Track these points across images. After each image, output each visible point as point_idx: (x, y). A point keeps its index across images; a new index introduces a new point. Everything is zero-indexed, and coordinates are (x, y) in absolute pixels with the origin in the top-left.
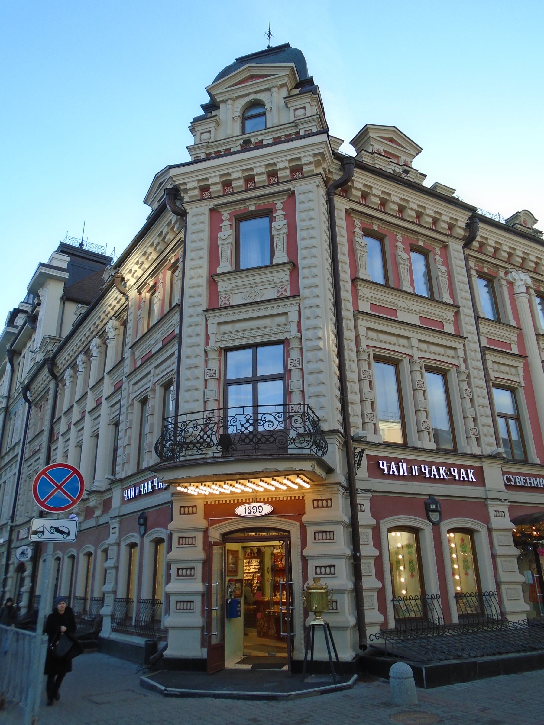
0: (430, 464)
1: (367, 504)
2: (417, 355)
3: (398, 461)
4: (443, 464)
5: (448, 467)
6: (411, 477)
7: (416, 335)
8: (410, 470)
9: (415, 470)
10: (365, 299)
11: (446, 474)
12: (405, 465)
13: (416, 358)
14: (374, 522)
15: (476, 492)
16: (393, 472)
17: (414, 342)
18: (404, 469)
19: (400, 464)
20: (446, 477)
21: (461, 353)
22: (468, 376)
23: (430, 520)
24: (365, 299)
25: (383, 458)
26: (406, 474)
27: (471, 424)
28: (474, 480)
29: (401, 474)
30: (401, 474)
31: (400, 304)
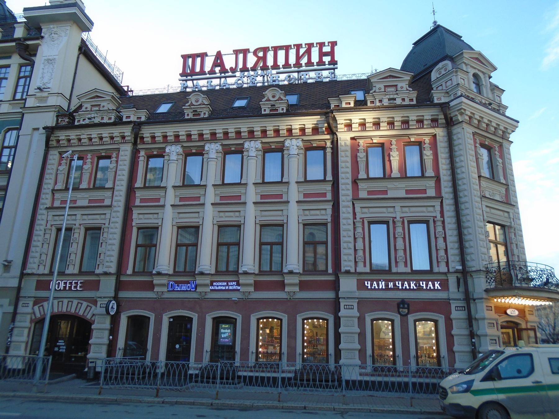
0: (403, 281)
1: (355, 305)
2: (398, 216)
3: (378, 281)
4: (413, 280)
5: (418, 281)
6: (387, 288)
7: (398, 204)
8: (387, 285)
9: (391, 285)
10: (364, 189)
11: (416, 286)
12: (383, 282)
13: (398, 218)
14: (358, 315)
15: (443, 295)
16: (375, 287)
17: (398, 209)
18: (382, 285)
19: (380, 282)
20: (415, 288)
21: (438, 208)
22: (443, 222)
23: (399, 313)
24: (364, 189)
25: (368, 280)
26: (384, 287)
27: (442, 253)
28: (439, 288)
29: (380, 287)
30: (380, 287)
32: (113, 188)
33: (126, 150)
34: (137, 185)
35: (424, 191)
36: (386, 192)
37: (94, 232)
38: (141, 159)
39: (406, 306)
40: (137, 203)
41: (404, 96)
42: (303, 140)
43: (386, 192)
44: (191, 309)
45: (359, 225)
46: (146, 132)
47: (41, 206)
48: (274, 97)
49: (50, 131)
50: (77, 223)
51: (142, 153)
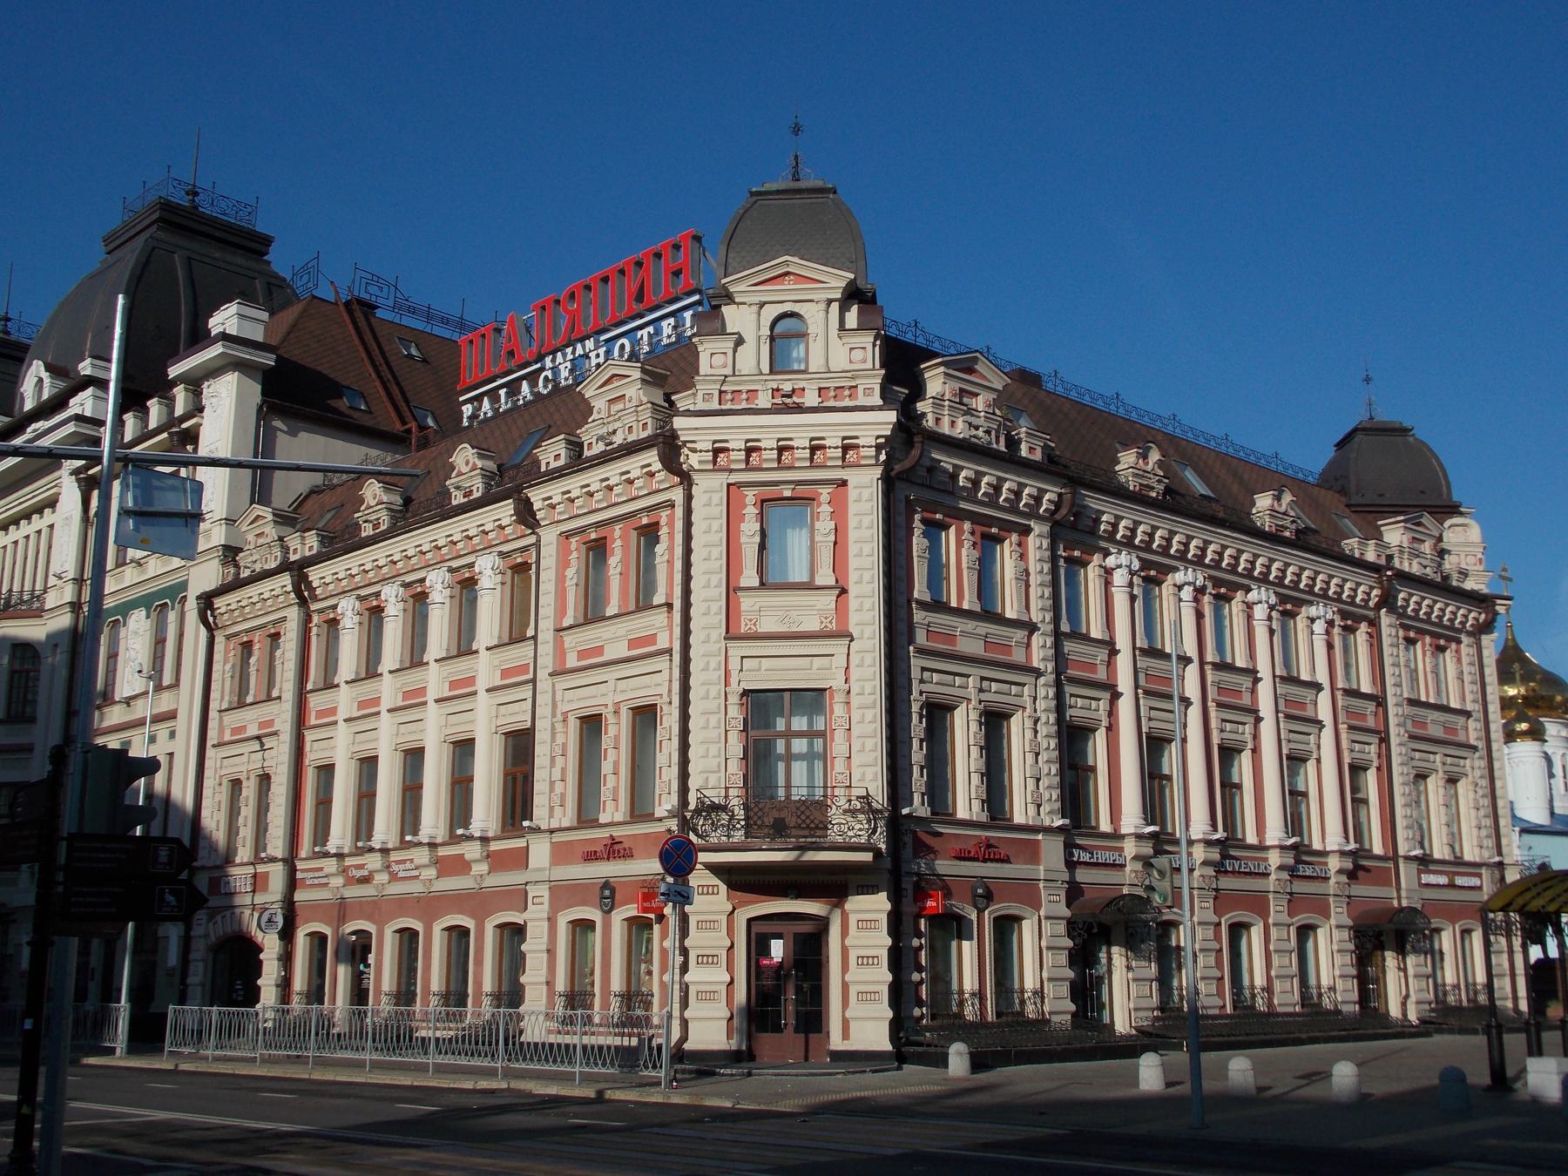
31: (606, 635)
32: (279, 698)
33: (293, 614)
34: (310, 686)
35: (651, 639)
36: (599, 650)
37: (265, 779)
38: (314, 630)
39: (607, 893)
40: (313, 720)
41: (629, 420)
42: (501, 554)
43: (599, 650)
44: (370, 918)
45: (559, 727)
46: (315, 574)
47: (209, 744)
48: (467, 463)
49: (207, 600)
50: (244, 768)
51: (315, 619)
